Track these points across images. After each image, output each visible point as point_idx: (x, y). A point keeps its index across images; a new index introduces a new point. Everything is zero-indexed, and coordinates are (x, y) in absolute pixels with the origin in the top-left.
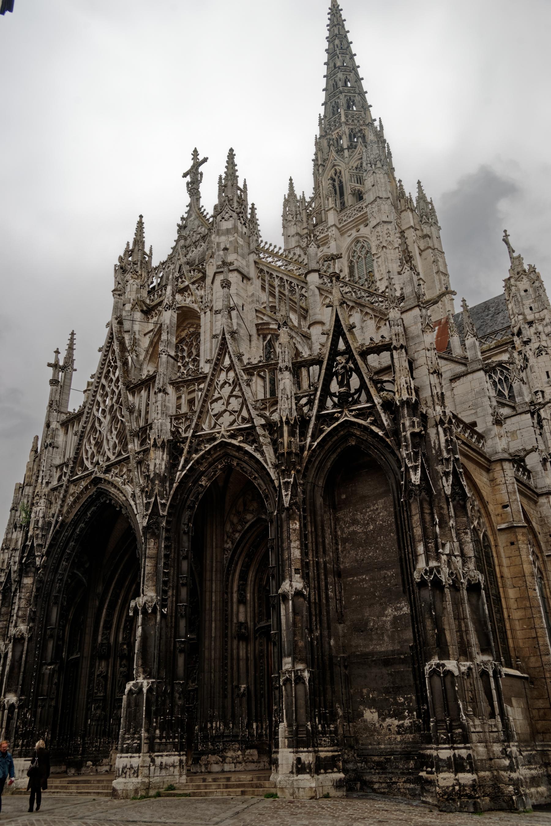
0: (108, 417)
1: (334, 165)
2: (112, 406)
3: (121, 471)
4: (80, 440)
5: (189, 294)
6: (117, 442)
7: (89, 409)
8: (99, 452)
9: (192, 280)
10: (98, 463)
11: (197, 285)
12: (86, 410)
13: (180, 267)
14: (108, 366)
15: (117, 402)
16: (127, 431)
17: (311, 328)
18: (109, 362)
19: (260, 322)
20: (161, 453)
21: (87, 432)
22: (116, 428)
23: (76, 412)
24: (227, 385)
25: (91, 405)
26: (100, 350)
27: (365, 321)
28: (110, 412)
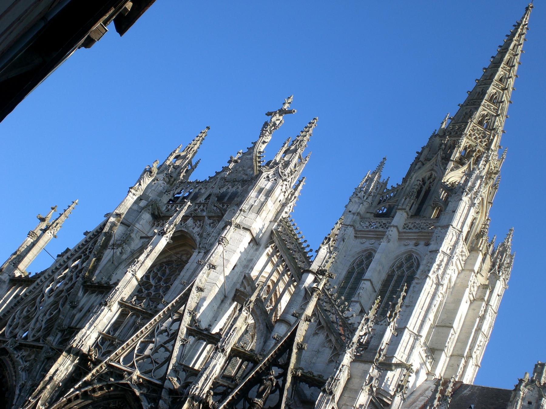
0: (52, 299)
1: (432, 170)
2: (62, 291)
3: (29, 356)
4: (15, 305)
5: (200, 225)
6: (43, 327)
7: (41, 281)
8: (23, 326)
9: (211, 214)
10: (15, 336)
11: (211, 221)
12: (38, 281)
13: (210, 195)
14: (83, 252)
15: (68, 290)
16: (57, 323)
17: (277, 324)
18: (86, 250)
19: (242, 289)
20: (69, 362)
21: (25, 302)
22: (51, 314)
23: (30, 276)
24: (166, 334)
25: (45, 278)
26: (86, 233)
27: (325, 346)
28: (57, 295)
